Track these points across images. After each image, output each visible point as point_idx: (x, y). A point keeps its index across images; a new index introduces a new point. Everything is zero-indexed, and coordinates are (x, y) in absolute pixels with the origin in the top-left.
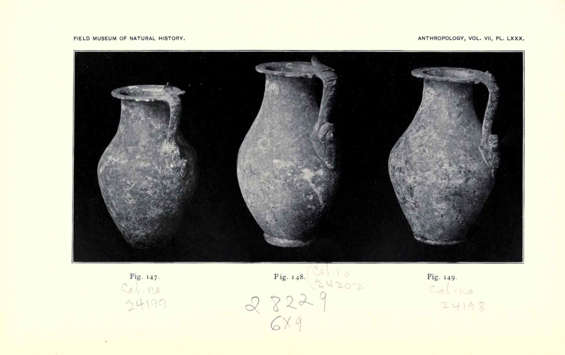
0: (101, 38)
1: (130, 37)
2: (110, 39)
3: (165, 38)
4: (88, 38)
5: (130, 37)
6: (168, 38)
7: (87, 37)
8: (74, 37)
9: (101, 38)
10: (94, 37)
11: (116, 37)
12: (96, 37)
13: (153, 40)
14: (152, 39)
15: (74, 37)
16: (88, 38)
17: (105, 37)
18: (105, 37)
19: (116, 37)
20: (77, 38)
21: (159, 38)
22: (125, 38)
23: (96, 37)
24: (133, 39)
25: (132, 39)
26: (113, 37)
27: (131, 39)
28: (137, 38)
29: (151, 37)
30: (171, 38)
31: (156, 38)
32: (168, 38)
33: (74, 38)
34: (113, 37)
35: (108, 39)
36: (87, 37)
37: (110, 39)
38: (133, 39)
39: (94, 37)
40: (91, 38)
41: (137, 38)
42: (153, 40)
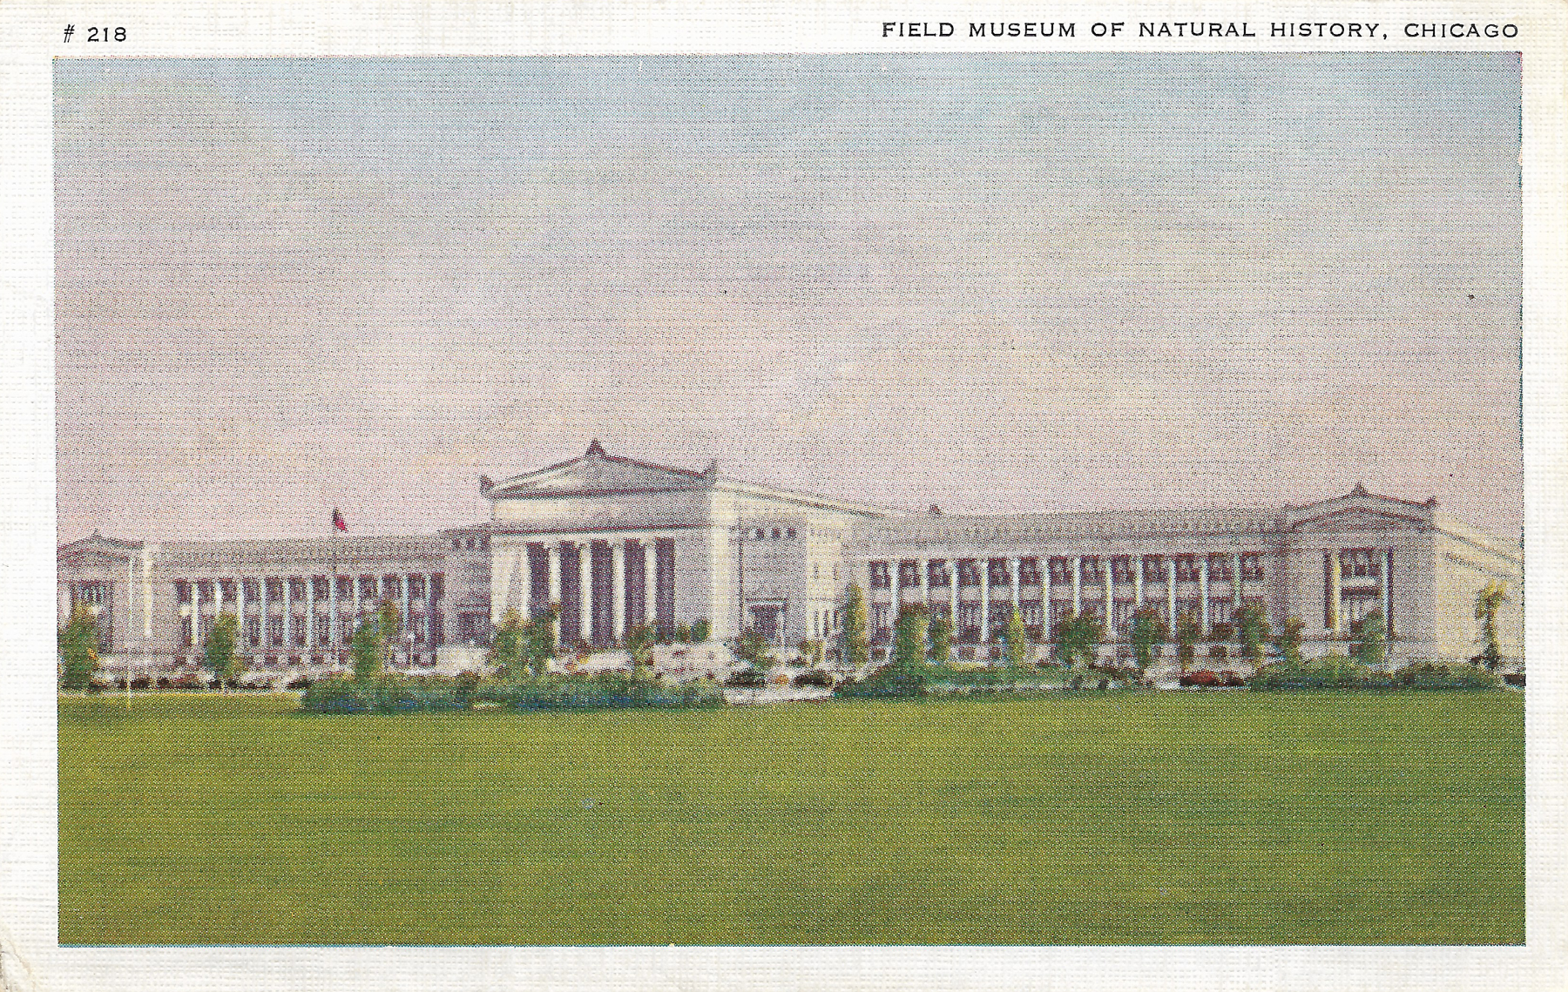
0: (1007, 31)
1: (1142, 25)
2: (1047, 30)
3: (1296, 27)
4: (946, 30)
5: (1142, 25)
6: (1315, 30)
7: (941, 24)
8: (885, 25)
9: (1007, 31)
10: (972, 25)
11: (1072, 26)
12: (983, 25)
13: (1245, 35)
14: (1241, 32)
15: (885, 25)
16: (947, 30)
17: (1026, 24)
18: (1026, 24)
19: (1072, 26)
20: (897, 28)
21: (1274, 29)
22: (1114, 29)
23: (983, 25)
24: (1156, 30)
25: (1152, 34)
26: (1062, 25)
27: (1145, 32)
28: (1175, 30)
29: (1232, 25)
30: (1326, 30)
31: (1260, 26)
32: (1315, 30)
33: (886, 28)
34: (1062, 25)
35: (1037, 30)
36: (941, 24)
37: (1047, 30)
38: (1156, 33)
39: (972, 25)
40: (962, 29)
41: (1175, 30)
42: (1241, 37)
